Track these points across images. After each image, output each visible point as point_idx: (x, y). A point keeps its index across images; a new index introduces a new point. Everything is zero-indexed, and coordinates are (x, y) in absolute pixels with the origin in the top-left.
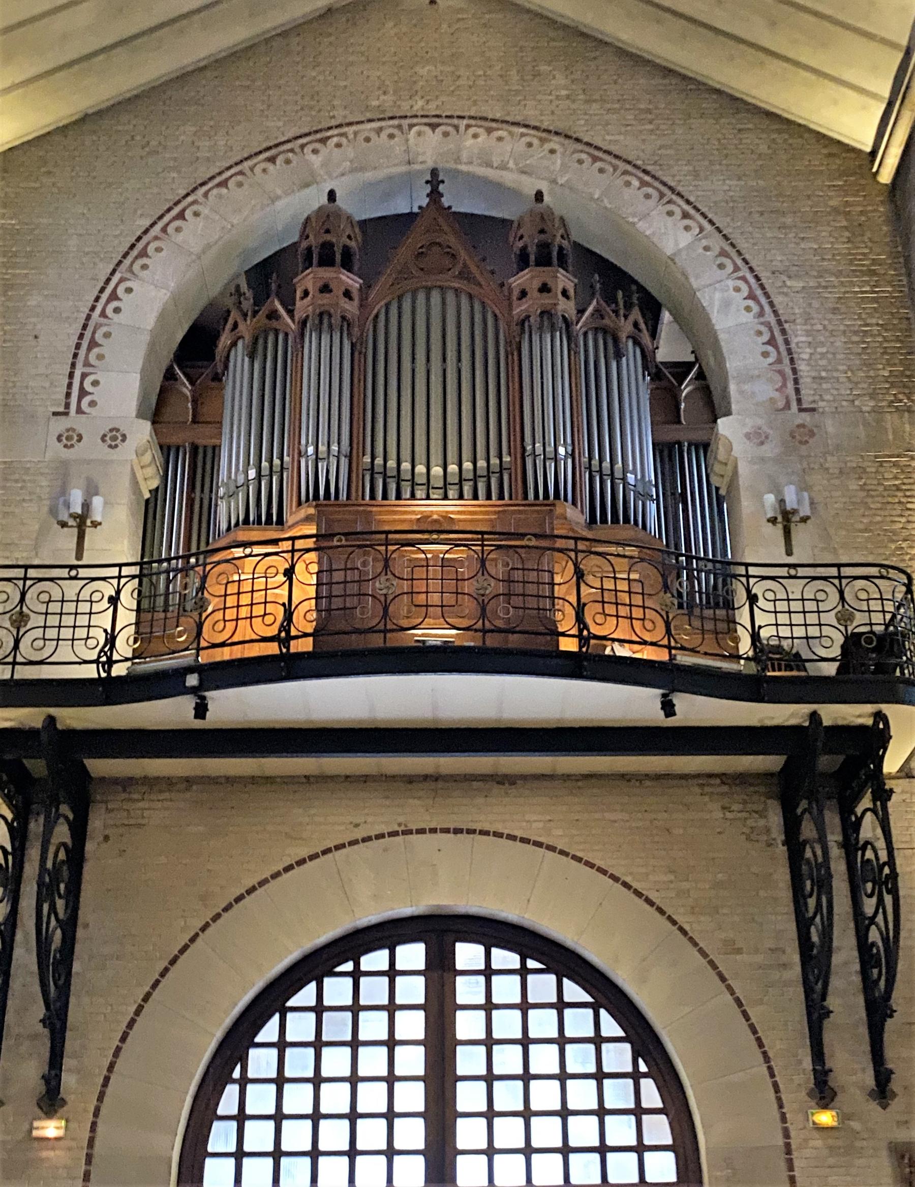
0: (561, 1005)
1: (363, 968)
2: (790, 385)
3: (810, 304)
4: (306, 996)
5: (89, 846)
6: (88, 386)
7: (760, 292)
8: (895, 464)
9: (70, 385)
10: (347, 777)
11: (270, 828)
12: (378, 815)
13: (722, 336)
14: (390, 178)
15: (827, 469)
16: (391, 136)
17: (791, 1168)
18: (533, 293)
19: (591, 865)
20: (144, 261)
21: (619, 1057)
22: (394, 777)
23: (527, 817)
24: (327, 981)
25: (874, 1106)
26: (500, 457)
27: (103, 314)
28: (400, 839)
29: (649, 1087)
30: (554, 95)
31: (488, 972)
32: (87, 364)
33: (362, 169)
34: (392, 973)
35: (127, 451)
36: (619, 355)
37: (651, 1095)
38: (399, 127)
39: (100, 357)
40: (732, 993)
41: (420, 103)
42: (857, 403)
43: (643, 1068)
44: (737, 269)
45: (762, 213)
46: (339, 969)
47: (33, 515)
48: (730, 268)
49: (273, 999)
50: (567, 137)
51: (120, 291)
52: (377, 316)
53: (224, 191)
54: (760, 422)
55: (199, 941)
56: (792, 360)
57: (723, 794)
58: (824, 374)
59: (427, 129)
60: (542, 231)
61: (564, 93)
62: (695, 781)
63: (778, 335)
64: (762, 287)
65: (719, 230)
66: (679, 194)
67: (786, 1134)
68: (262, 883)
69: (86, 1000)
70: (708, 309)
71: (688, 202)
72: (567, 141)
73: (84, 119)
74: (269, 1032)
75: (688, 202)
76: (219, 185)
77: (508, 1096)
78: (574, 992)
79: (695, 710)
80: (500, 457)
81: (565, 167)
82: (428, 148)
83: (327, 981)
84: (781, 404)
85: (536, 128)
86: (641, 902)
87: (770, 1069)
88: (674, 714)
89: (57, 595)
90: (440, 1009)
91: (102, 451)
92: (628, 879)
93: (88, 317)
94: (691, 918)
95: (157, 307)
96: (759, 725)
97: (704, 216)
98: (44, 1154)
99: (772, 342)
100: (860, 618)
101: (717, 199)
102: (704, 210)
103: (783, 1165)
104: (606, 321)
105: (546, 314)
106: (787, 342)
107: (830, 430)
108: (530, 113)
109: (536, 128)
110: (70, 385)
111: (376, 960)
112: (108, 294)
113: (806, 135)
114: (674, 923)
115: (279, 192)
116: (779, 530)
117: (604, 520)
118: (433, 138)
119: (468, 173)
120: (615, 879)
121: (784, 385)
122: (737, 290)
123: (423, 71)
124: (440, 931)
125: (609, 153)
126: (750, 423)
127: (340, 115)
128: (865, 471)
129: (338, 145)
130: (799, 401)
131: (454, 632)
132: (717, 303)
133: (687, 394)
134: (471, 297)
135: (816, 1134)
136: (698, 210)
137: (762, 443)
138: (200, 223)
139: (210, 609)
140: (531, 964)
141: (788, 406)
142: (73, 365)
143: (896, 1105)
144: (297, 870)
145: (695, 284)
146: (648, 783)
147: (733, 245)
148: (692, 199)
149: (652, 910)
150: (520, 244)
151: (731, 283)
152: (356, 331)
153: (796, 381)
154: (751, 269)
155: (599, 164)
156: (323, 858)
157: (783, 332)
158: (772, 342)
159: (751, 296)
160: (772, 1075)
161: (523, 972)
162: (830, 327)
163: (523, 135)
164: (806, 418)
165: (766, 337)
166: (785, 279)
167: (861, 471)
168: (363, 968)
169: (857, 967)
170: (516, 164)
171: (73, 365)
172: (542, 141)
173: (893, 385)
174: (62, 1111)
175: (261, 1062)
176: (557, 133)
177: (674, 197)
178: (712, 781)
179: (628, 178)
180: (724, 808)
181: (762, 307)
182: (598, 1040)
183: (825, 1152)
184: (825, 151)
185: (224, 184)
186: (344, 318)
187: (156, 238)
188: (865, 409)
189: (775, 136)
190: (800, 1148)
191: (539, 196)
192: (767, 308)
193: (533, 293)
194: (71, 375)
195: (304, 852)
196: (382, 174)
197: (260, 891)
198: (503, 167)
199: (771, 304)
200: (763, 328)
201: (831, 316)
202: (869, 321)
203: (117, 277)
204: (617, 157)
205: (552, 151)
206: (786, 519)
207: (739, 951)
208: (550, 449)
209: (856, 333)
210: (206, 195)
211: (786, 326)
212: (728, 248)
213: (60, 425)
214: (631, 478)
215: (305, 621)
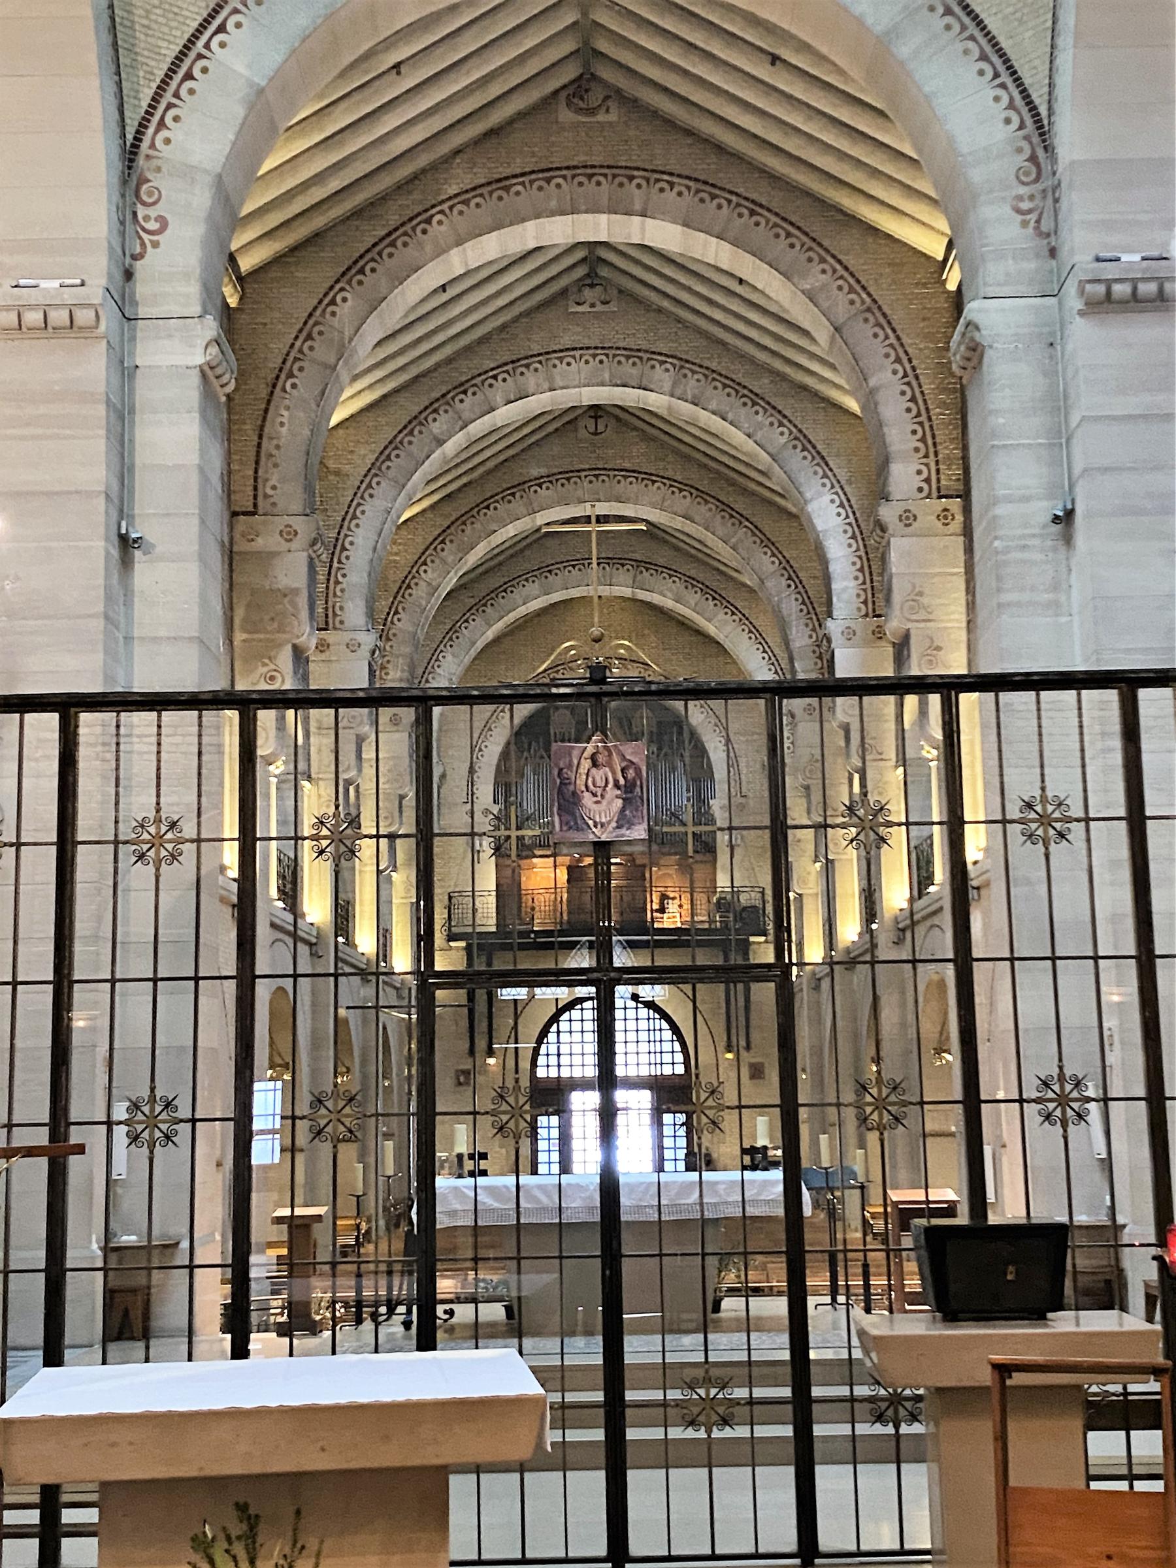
4: (566, 1016)
74: (554, 1028)
77: (632, 1047)
133: (701, 775)
175: (552, 1037)
215: (565, 917)
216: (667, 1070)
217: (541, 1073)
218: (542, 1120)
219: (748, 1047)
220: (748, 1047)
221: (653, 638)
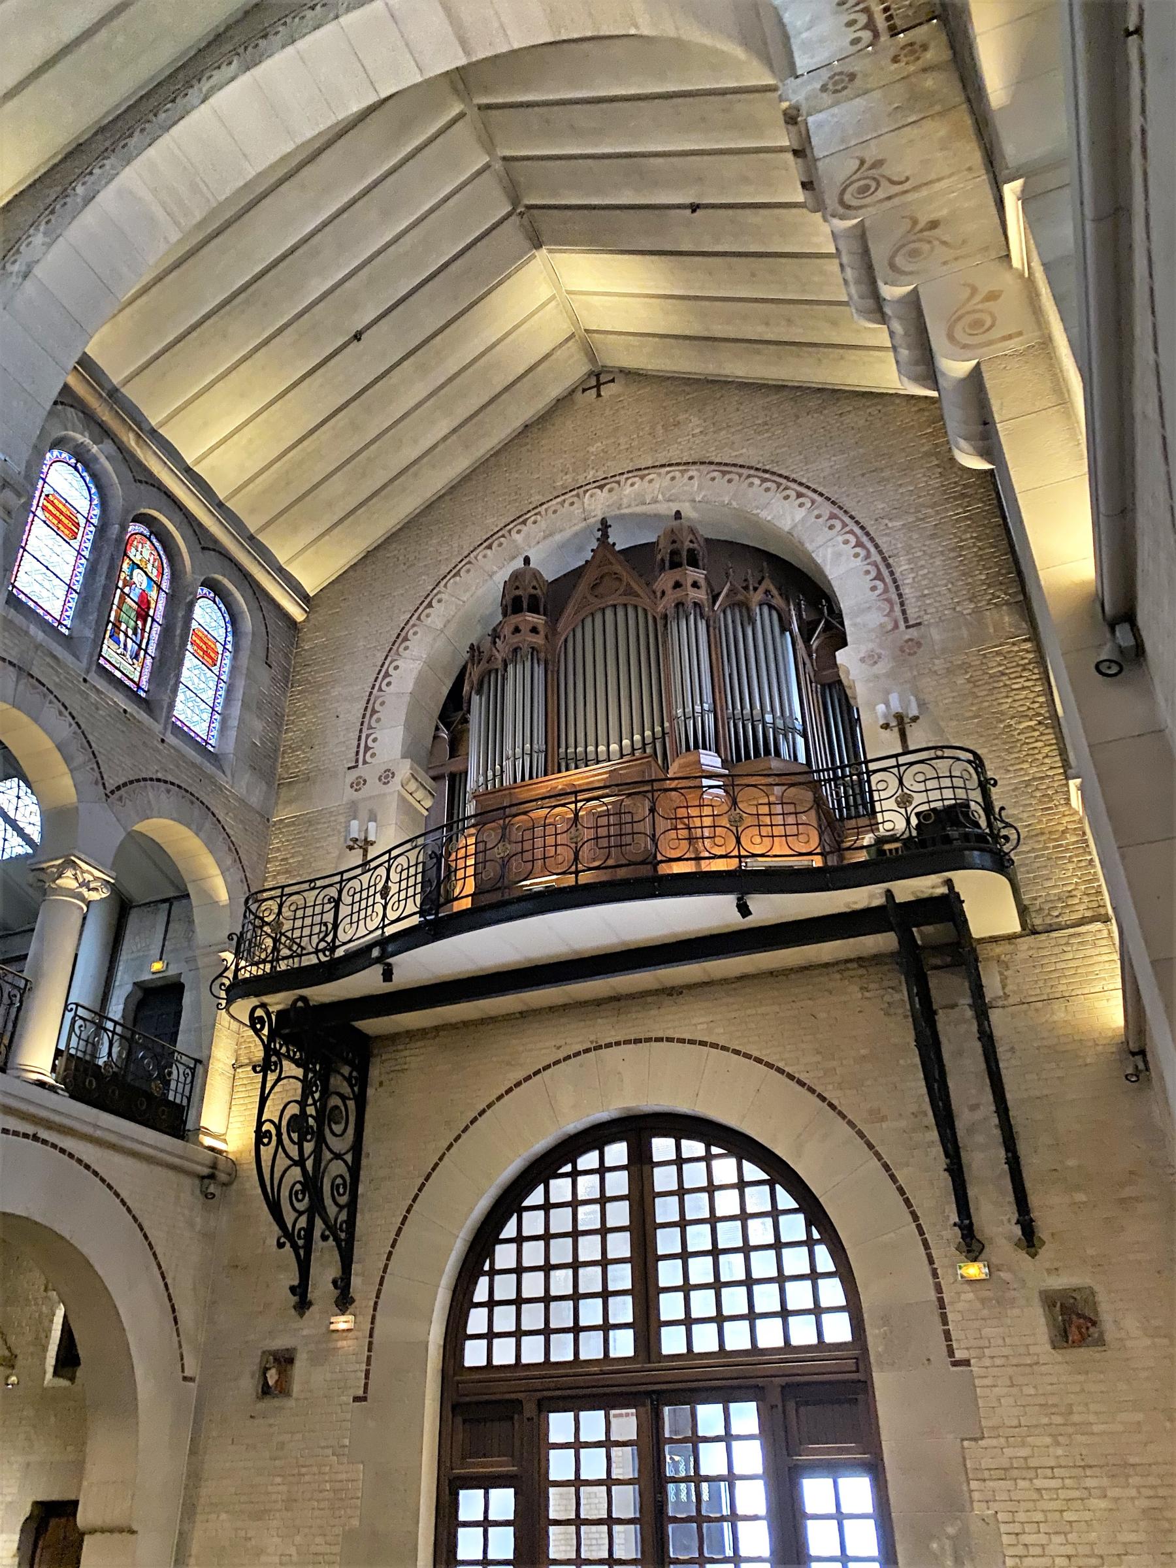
0: (742, 1185)
1: (580, 1167)
2: (897, 608)
3: (910, 538)
5: (370, 1092)
6: (370, 743)
7: (865, 537)
8: (998, 653)
9: (359, 746)
10: (551, 1008)
11: (494, 1059)
12: (575, 1036)
13: (836, 585)
14: (576, 534)
15: (935, 672)
16: (572, 504)
17: (945, 1321)
18: (669, 591)
19: (747, 1056)
20: (407, 643)
21: (794, 1227)
22: (585, 1002)
23: (694, 1022)
24: (553, 1182)
25: (1023, 1255)
26: (662, 726)
27: (380, 689)
28: (593, 1053)
29: (822, 1251)
30: (693, 433)
31: (680, 1161)
32: (370, 728)
33: (551, 535)
34: (602, 1170)
35: (395, 785)
36: (752, 622)
37: (824, 1261)
38: (578, 495)
39: (378, 720)
40: (880, 1158)
41: (592, 473)
42: (958, 609)
43: (816, 1235)
44: (845, 525)
45: (863, 475)
46: (561, 1171)
47: (335, 843)
48: (838, 525)
49: (509, 1202)
50: (702, 463)
51: (391, 671)
52: (566, 641)
53: (458, 578)
54: (871, 646)
55: (445, 1159)
56: (897, 588)
57: (861, 976)
58: (926, 592)
59: (598, 491)
60: (674, 542)
61: (697, 431)
62: (836, 968)
63: (884, 570)
64: (867, 534)
65: (828, 499)
66: (794, 481)
67: (939, 1289)
68: (489, 1106)
69: (367, 1216)
70: (822, 565)
71: (801, 484)
72: (702, 467)
73: (369, 556)
75: (801, 484)
76: (454, 576)
78: (752, 1172)
79: (770, 908)
80: (662, 726)
81: (700, 488)
82: (598, 504)
83: (553, 1182)
84: (890, 627)
85: (678, 464)
86: (793, 1084)
87: (919, 1227)
88: (750, 913)
89: (301, 903)
90: (642, 1198)
91: (379, 788)
92: (781, 1065)
93: (371, 693)
94: (839, 1093)
95: (415, 674)
96: (848, 910)
97: (815, 491)
98: (340, 1344)
99: (879, 577)
100: (918, 798)
101: (826, 474)
102: (813, 486)
103: (937, 1319)
104: (740, 597)
105: (679, 605)
106: (892, 573)
107: (936, 637)
108: (674, 454)
109: (678, 464)
110: (359, 746)
111: (589, 1160)
112: (383, 673)
113: (898, 401)
114: (823, 1099)
115: (495, 568)
116: (895, 734)
117: (748, 757)
118: (602, 495)
119: (631, 514)
120: (770, 1065)
121: (892, 610)
122: (846, 542)
123: (592, 449)
124: (637, 1129)
125: (735, 465)
126: (864, 649)
127: (537, 499)
128: (971, 666)
129: (535, 522)
130: (906, 620)
131: (555, 877)
132: (829, 556)
134: (636, 607)
135: (967, 1287)
136: (808, 487)
137: (876, 663)
138: (443, 604)
139: (391, 894)
140: (715, 1150)
141: (896, 626)
142: (361, 731)
143: (1044, 1253)
144: (516, 1091)
145: (809, 547)
146: (793, 976)
147: (841, 508)
148: (804, 481)
149: (804, 1091)
150: (659, 557)
151: (840, 539)
152: (542, 655)
153: (902, 604)
154: (857, 523)
155: (728, 477)
156: (535, 1079)
157: (888, 566)
158: (879, 577)
159: (859, 544)
160: (922, 1233)
161: (708, 1158)
162: (929, 552)
163: (668, 472)
164: (913, 633)
165: (873, 574)
166: (887, 521)
167: (965, 667)
168: (580, 1167)
169: (996, 1121)
170: (663, 496)
171: (361, 731)
172: (683, 472)
173: (989, 586)
174: (351, 1309)
176: (694, 463)
177: (790, 484)
178: (849, 965)
179: (751, 480)
180: (861, 988)
181: (868, 551)
182: (775, 1213)
183: (978, 1305)
184: (913, 409)
185: (458, 574)
186: (533, 648)
187: (414, 625)
188: (965, 612)
189: (869, 410)
190: (952, 1303)
191: (678, 515)
192: (873, 550)
193: (669, 591)
194: (360, 738)
195: (520, 1075)
196: (568, 534)
197: (489, 1113)
198: (655, 501)
199: (877, 546)
200: (869, 567)
201: (927, 543)
202: (963, 537)
203: (389, 659)
204: (741, 466)
205: (691, 478)
206: (901, 723)
207: (883, 1119)
208: (689, 709)
209: (953, 550)
210: (445, 586)
211: (891, 561)
212: (836, 511)
213: (352, 776)
214: (769, 718)
216: (803, 1333)
217: (474, 1355)
218: (470, 1503)
219: (1029, 1238)
220: (1029, 1238)
221: (695, 420)
